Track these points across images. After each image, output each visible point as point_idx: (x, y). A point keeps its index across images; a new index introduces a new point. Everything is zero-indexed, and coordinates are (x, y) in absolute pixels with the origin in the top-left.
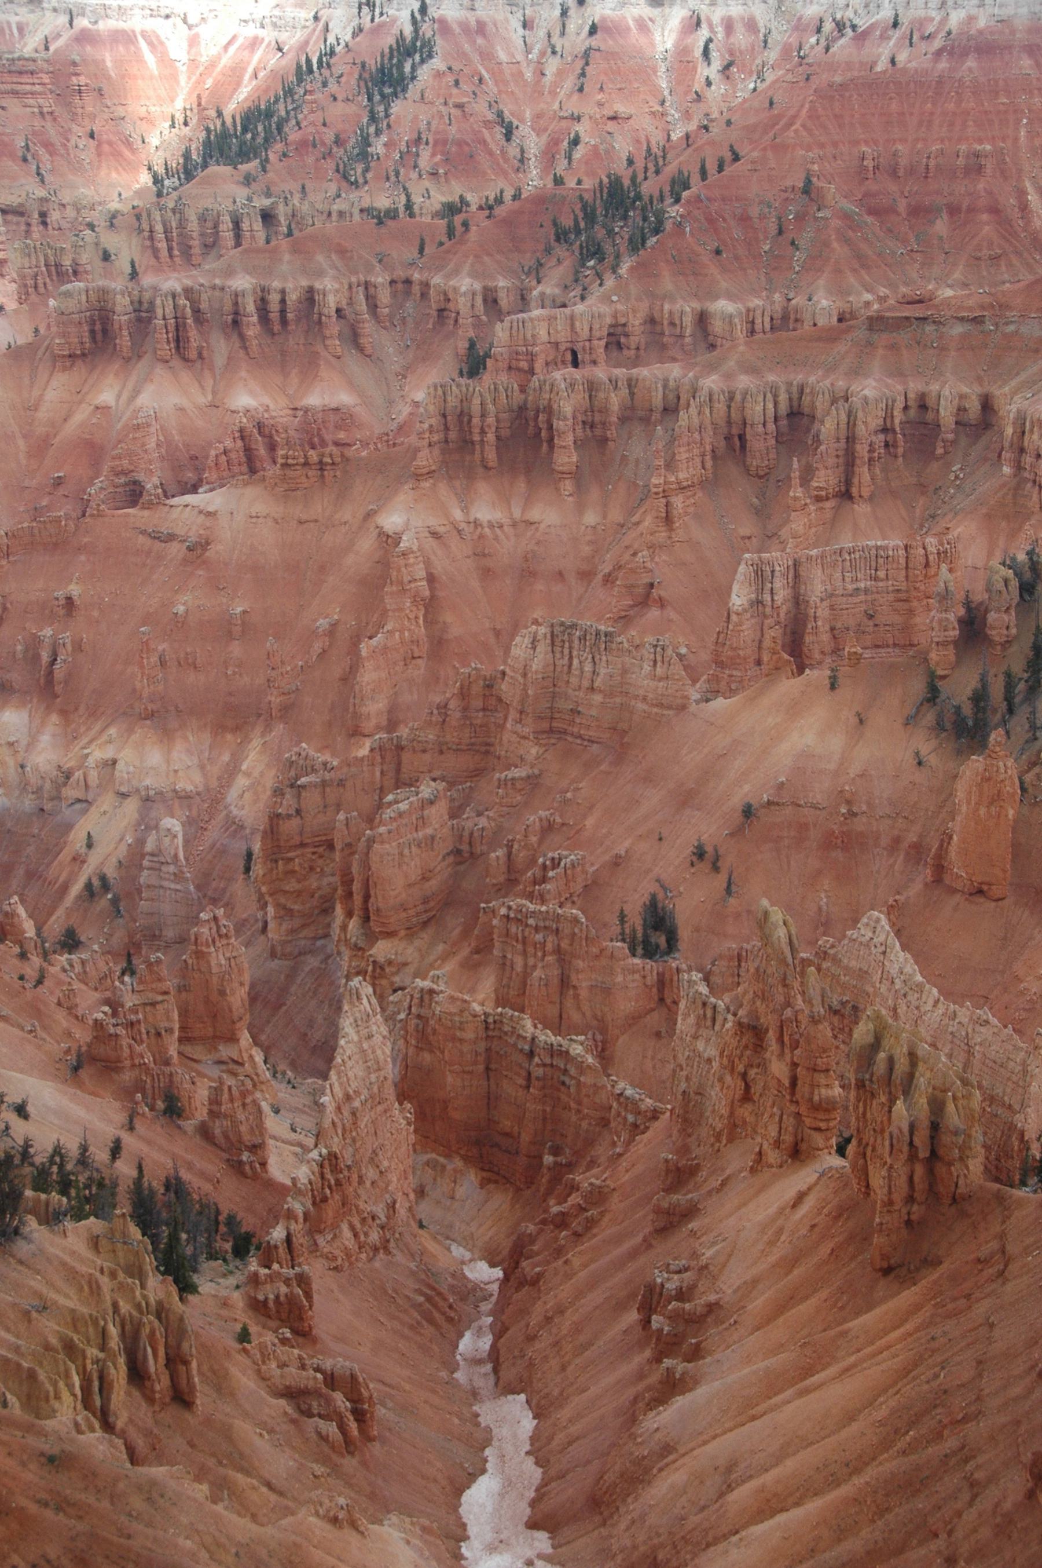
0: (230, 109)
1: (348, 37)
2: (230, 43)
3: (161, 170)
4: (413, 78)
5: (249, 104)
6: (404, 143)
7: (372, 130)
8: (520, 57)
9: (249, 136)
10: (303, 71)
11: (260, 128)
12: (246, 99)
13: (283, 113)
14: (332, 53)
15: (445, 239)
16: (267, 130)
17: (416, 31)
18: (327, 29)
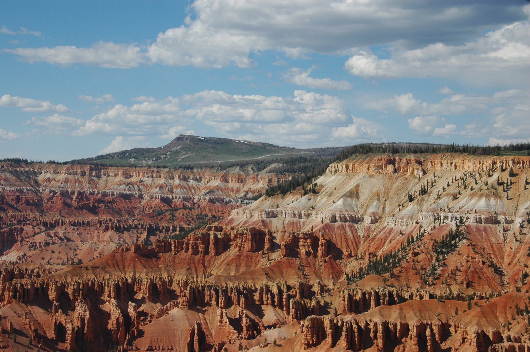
0: (380, 253)
1: (429, 230)
3: (350, 275)
4: (456, 247)
5: (387, 252)
6: (450, 271)
7: (437, 264)
8: (500, 242)
9: (386, 264)
10: (410, 242)
11: (391, 261)
12: (386, 250)
13: (401, 256)
14: (422, 235)
15: (467, 309)
16: (394, 262)
17: (458, 229)
18: (421, 227)
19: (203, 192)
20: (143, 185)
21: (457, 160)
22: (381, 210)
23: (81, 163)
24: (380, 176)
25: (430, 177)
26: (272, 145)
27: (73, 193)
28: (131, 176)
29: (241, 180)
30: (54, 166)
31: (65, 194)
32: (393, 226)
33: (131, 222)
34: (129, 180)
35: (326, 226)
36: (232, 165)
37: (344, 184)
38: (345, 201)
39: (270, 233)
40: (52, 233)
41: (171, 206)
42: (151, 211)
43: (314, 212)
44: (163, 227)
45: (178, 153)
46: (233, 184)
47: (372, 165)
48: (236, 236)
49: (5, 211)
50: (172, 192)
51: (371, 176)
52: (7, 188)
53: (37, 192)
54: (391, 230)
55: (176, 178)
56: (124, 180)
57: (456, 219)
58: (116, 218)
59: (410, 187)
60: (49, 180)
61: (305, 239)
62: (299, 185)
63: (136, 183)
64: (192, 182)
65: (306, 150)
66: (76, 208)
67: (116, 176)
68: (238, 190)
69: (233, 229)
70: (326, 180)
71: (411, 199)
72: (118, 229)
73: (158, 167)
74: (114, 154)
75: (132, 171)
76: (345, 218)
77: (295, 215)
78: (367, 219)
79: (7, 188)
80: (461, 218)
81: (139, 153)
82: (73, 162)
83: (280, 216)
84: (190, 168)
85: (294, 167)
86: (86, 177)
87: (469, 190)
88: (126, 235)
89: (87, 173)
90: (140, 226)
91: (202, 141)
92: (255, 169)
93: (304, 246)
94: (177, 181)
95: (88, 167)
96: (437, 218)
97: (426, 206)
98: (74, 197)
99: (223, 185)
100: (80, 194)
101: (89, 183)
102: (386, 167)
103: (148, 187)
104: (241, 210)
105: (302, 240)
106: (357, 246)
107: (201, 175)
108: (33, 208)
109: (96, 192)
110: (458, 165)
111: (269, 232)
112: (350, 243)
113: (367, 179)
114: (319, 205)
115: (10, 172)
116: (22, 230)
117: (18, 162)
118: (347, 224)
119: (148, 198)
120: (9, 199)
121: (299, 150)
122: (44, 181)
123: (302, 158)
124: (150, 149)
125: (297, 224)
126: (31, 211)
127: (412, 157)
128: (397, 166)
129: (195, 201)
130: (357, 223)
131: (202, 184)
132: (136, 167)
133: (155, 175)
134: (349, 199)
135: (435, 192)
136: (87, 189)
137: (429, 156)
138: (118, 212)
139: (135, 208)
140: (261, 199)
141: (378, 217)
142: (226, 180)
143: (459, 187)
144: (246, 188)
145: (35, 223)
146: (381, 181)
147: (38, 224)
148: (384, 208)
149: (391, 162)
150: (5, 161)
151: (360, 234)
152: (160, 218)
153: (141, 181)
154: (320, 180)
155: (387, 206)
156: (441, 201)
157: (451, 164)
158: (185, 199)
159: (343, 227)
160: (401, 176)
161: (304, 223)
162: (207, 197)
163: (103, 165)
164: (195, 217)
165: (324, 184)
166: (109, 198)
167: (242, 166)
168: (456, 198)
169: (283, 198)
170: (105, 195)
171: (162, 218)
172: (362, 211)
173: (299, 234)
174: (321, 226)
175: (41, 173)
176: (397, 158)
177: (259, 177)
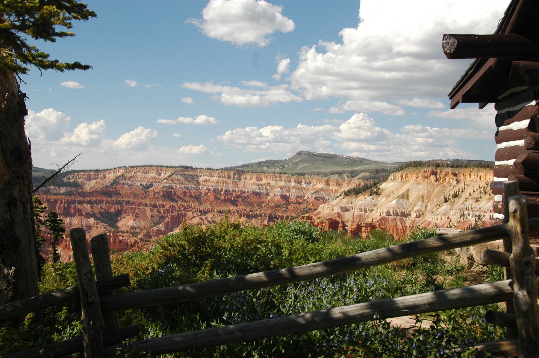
2: (423, 223)
19: (311, 192)
20: (269, 186)
21: (482, 174)
22: (424, 208)
23: (230, 169)
24: (426, 183)
25: (461, 185)
26: (366, 160)
27: (222, 190)
28: (261, 179)
29: (339, 184)
30: (209, 171)
31: (216, 192)
32: (431, 220)
33: (259, 212)
34: (260, 183)
35: (383, 219)
36: (333, 173)
37: (399, 189)
38: (398, 200)
39: (343, 223)
40: (203, 217)
41: (288, 201)
42: (273, 204)
43: (375, 208)
44: (279, 216)
45: (298, 163)
46: (333, 187)
47: (419, 176)
48: (318, 223)
49: (176, 201)
50: (289, 191)
51: (419, 183)
52: (178, 186)
53: (198, 189)
54: (429, 223)
55: (293, 181)
56: (257, 182)
57: (476, 216)
58: (249, 208)
59: (446, 192)
60: (206, 181)
61: (366, 227)
62: (368, 188)
63: (264, 184)
64: (304, 185)
65: (391, 164)
66: (222, 201)
67: (251, 179)
68: (336, 191)
69: (319, 218)
70: (386, 186)
71: (446, 201)
72: (248, 216)
73: (280, 173)
74: (254, 164)
75: (262, 176)
76: (397, 213)
77: (361, 210)
78: (413, 215)
79: (178, 186)
80: (479, 215)
81: (270, 163)
82: (226, 169)
83: (351, 210)
84: (303, 175)
85: (377, 176)
86: (231, 179)
87: (488, 195)
88: (253, 221)
89: (232, 177)
90: (263, 215)
91: (315, 155)
92: (349, 176)
93: (365, 232)
94: (293, 184)
95: (232, 173)
96: (463, 215)
97: (456, 206)
98: (222, 193)
99: (325, 187)
100: (226, 191)
101: (233, 184)
102: (430, 177)
103: (273, 187)
104: (325, 205)
105: (364, 228)
106: (404, 234)
107: (310, 180)
108: (195, 200)
109: (237, 190)
110: (482, 177)
111: (341, 221)
112: (399, 231)
113: (415, 185)
114: (380, 203)
115: (181, 175)
116: (185, 214)
117: (186, 168)
118: (398, 217)
119: (272, 195)
120: (179, 194)
121: (386, 163)
122: (203, 182)
123: (384, 169)
124: (278, 161)
125: (363, 216)
126: (193, 202)
127: (449, 170)
128: (438, 176)
129: (305, 198)
130: (406, 217)
131: (311, 186)
132: (265, 173)
133: (278, 179)
134: (401, 200)
135: (463, 196)
136: (231, 188)
137: (462, 170)
138: (251, 204)
139: (263, 202)
140: (340, 198)
141: (421, 213)
142: (327, 184)
143: (481, 193)
144: (342, 190)
145: (194, 210)
146: (426, 187)
147: (196, 211)
148: (426, 207)
149: (434, 173)
150: (178, 167)
151: (408, 225)
152: (277, 209)
153: (268, 183)
154: (383, 186)
155: (429, 205)
156: (467, 203)
157: (478, 176)
158: (298, 197)
159: (395, 220)
160: (441, 184)
161: (368, 216)
162: (314, 196)
163: (243, 171)
164: (302, 209)
165: (384, 188)
166: (246, 194)
167: (340, 174)
168: (478, 201)
169: (356, 197)
170: (244, 192)
171: (279, 210)
172: (410, 209)
173: (361, 224)
174: (379, 218)
175: (201, 176)
176: (439, 171)
177: (352, 182)
